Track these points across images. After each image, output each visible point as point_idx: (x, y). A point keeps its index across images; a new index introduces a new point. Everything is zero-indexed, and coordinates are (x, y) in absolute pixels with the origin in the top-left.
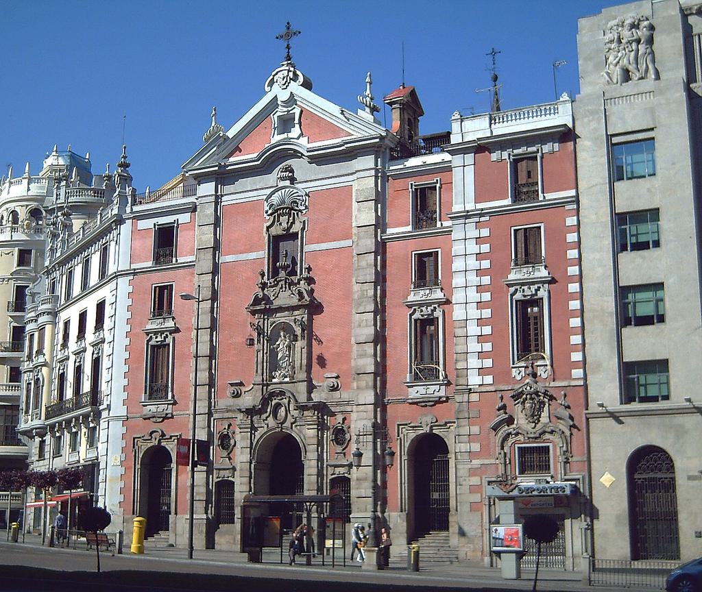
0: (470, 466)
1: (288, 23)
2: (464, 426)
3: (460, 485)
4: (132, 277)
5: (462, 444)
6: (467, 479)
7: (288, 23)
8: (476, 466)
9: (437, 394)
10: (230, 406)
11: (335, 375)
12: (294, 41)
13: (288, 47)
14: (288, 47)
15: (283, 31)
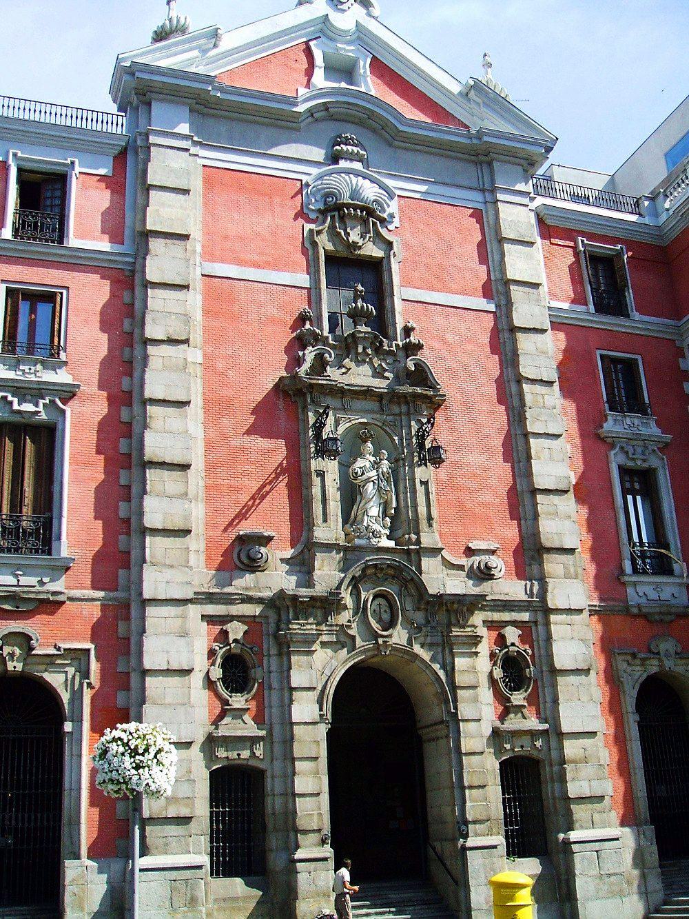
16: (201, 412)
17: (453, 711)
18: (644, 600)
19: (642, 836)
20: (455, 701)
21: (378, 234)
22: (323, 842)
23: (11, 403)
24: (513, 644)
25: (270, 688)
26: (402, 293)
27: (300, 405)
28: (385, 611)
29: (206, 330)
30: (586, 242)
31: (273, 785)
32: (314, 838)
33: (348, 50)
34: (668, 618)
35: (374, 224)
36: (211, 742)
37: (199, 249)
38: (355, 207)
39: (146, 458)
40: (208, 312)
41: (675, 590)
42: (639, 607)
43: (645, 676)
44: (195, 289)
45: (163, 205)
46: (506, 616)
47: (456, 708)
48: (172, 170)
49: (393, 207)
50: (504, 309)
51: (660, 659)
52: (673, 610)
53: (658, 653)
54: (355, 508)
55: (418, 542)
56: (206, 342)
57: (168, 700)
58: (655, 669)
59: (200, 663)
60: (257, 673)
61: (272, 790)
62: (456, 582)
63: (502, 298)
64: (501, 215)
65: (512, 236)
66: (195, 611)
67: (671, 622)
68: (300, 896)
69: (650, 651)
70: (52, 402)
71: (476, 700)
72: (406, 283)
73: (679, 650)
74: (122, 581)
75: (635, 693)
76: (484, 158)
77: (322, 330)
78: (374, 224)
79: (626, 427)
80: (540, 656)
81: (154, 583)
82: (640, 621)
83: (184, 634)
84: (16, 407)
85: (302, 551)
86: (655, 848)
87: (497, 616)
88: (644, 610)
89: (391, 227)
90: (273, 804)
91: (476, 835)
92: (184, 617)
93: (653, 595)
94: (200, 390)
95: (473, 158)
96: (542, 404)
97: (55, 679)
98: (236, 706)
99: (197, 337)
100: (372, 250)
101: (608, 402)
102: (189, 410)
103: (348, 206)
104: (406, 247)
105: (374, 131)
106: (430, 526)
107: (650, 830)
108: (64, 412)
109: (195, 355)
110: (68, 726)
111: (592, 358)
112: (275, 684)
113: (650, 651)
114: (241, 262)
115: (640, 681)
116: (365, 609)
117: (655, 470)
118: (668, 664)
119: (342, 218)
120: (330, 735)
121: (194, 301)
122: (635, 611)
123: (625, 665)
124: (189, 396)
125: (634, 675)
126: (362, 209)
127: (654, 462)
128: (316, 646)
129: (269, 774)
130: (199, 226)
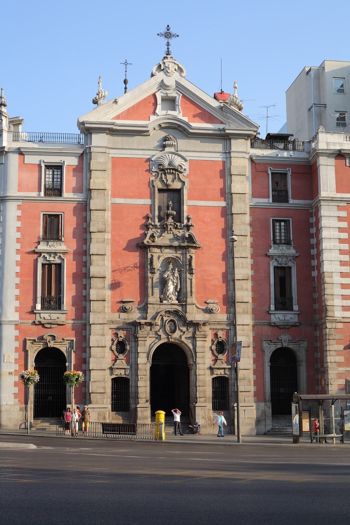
0: (337, 372)
1: (168, 26)
2: (333, 345)
3: (331, 384)
4: (20, 203)
5: (332, 357)
6: (336, 380)
7: (168, 26)
8: (342, 372)
9: (291, 320)
10: (125, 319)
11: (216, 301)
12: (172, 41)
13: (168, 44)
14: (168, 44)
15: (164, 30)
16: (110, 259)
17: (194, 361)
18: (278, 320)
19: (266, 406)
20: (196, 357)
21: (179, 179)
22: (147, 401)
23: (46, 258)
24: (220, 337)
25: (132, 352)
26: (187, 203)
27: (146, 252)
28: (173, 326)
29: (113, 225)
30: (272, 169)
31: (132, 383)
32: (144, 400)
33: (172, 93)
34: (288, 327)
35: (178, 174)
36: (111, 369)
37: (110, 193)
38: (170, 169)
39: (91, 276)
40: (113, 218)
41: (292, 316)
42: (274, 323)
43: (275, 349)
44: (108, 210)
45: (96, 178)
46: (219, 327)
47: (196, 360)
48: (100, 163)
49: (186, 166)
50: (230, 205)
51: (282, 343)
52: (290, 324)
53: (281, 340)
54: (165, 289)
55: (186, 301)
56: (112, 230)
57: (98, 357)
58: (280, 346)
59: (109, 344)
60: (128, 347)
61: (132, 385)
62: (201, 315)
63: (230, 200)
64: (232, 164)
65: (236, 173)
66: (106, 327)
67: (289, 328)
68: (138, 419)
69: (278, 340)
70: (60, 256)
71: (203, 357)
72: (189, 198)
73: (290, 339)
74: (84, 317)
75: (270, 355)
76: (227, 137)
77: (154, 222)
78: (178, 174)
79: (279, 250)
80: (231, 341)
81: (93, 318)
82: (276, 328)
83: (103, 335)
84: (48, 259)
85: (145, 305)
86: (270, 410)
87: (215, 327)
88: (276, 324)
89: (185, 174)
90: (132, 390)
91: (200, 402)
92: (103, 329)
93: (283, 318)
94: (110, 248)
95: (223, 138)
96: (241, 245)
97: (63, 349)
98: (120, 358)
99: (109, 228)
100: (177, 185)
101: (273, 240)
102: (106, 257)
103: (167, 169)
104: (191, 183)
105: (181, 131)
106: (191, 295)
107: (269, 404)
108: (64, 260)
109: (108, 236)
110: (67, 364)
111: (269, 222)
112: (133, 351)
113: (278, 340)
114: (125, 197)
115: (273, 351)
116: (165, 326)
117: (290, 268)
118: (285, 345)
119: (165, 174)
120: (151, 368)
121: (108, 214)
122: (273, 324)
123: (267, 344)
124: (105, 252)
125: (269, 349)
126: (173, 169)
127: (290, 264)
128: (148, 339)
129: (130, 380)
130: (110, 184)
